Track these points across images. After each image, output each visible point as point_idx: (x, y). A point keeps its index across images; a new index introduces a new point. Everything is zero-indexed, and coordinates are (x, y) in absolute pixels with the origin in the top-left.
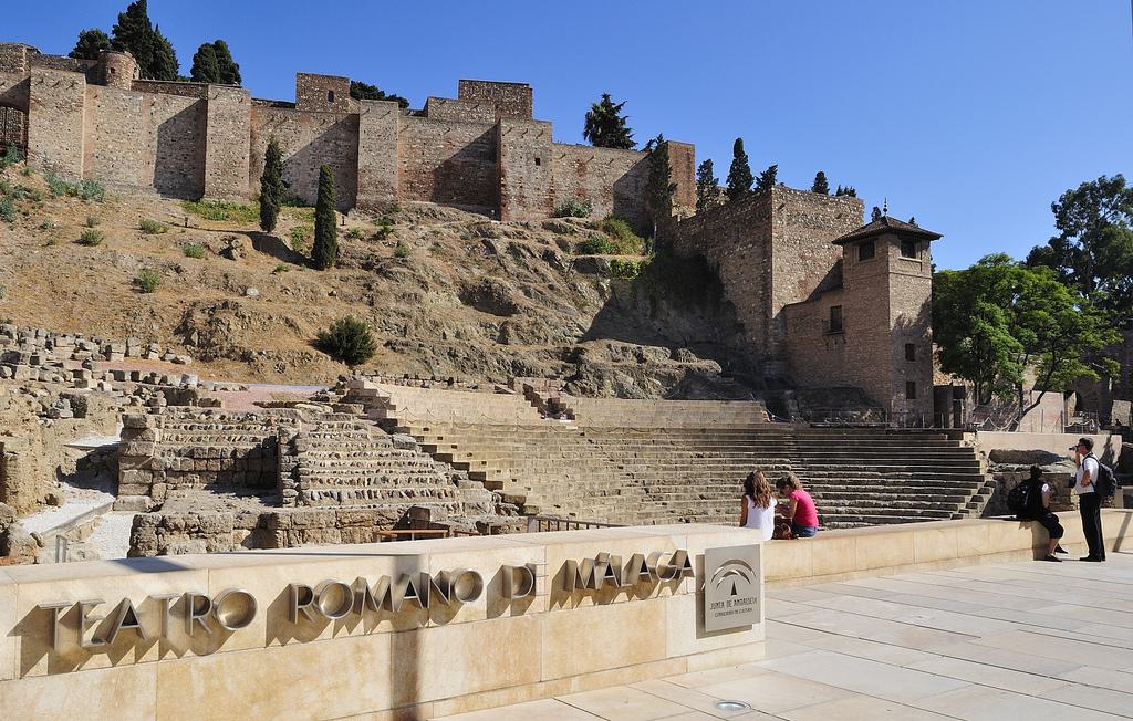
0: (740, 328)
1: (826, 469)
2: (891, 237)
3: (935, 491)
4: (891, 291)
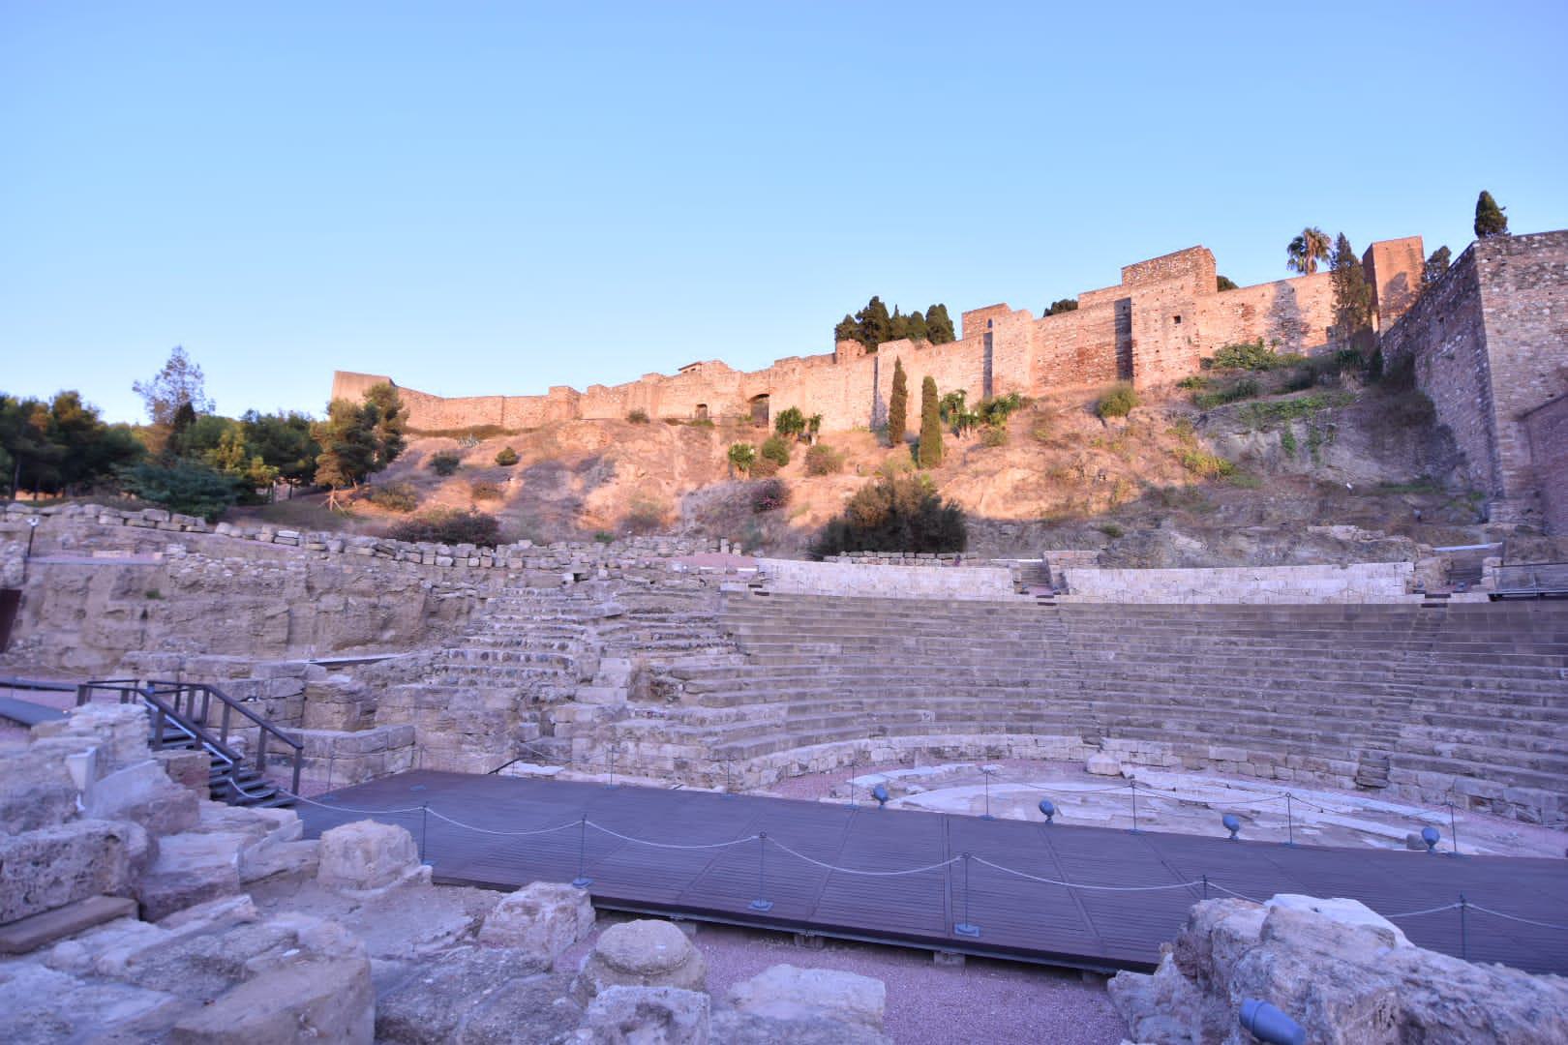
0: (1461, 460)
1: (1463, 672)
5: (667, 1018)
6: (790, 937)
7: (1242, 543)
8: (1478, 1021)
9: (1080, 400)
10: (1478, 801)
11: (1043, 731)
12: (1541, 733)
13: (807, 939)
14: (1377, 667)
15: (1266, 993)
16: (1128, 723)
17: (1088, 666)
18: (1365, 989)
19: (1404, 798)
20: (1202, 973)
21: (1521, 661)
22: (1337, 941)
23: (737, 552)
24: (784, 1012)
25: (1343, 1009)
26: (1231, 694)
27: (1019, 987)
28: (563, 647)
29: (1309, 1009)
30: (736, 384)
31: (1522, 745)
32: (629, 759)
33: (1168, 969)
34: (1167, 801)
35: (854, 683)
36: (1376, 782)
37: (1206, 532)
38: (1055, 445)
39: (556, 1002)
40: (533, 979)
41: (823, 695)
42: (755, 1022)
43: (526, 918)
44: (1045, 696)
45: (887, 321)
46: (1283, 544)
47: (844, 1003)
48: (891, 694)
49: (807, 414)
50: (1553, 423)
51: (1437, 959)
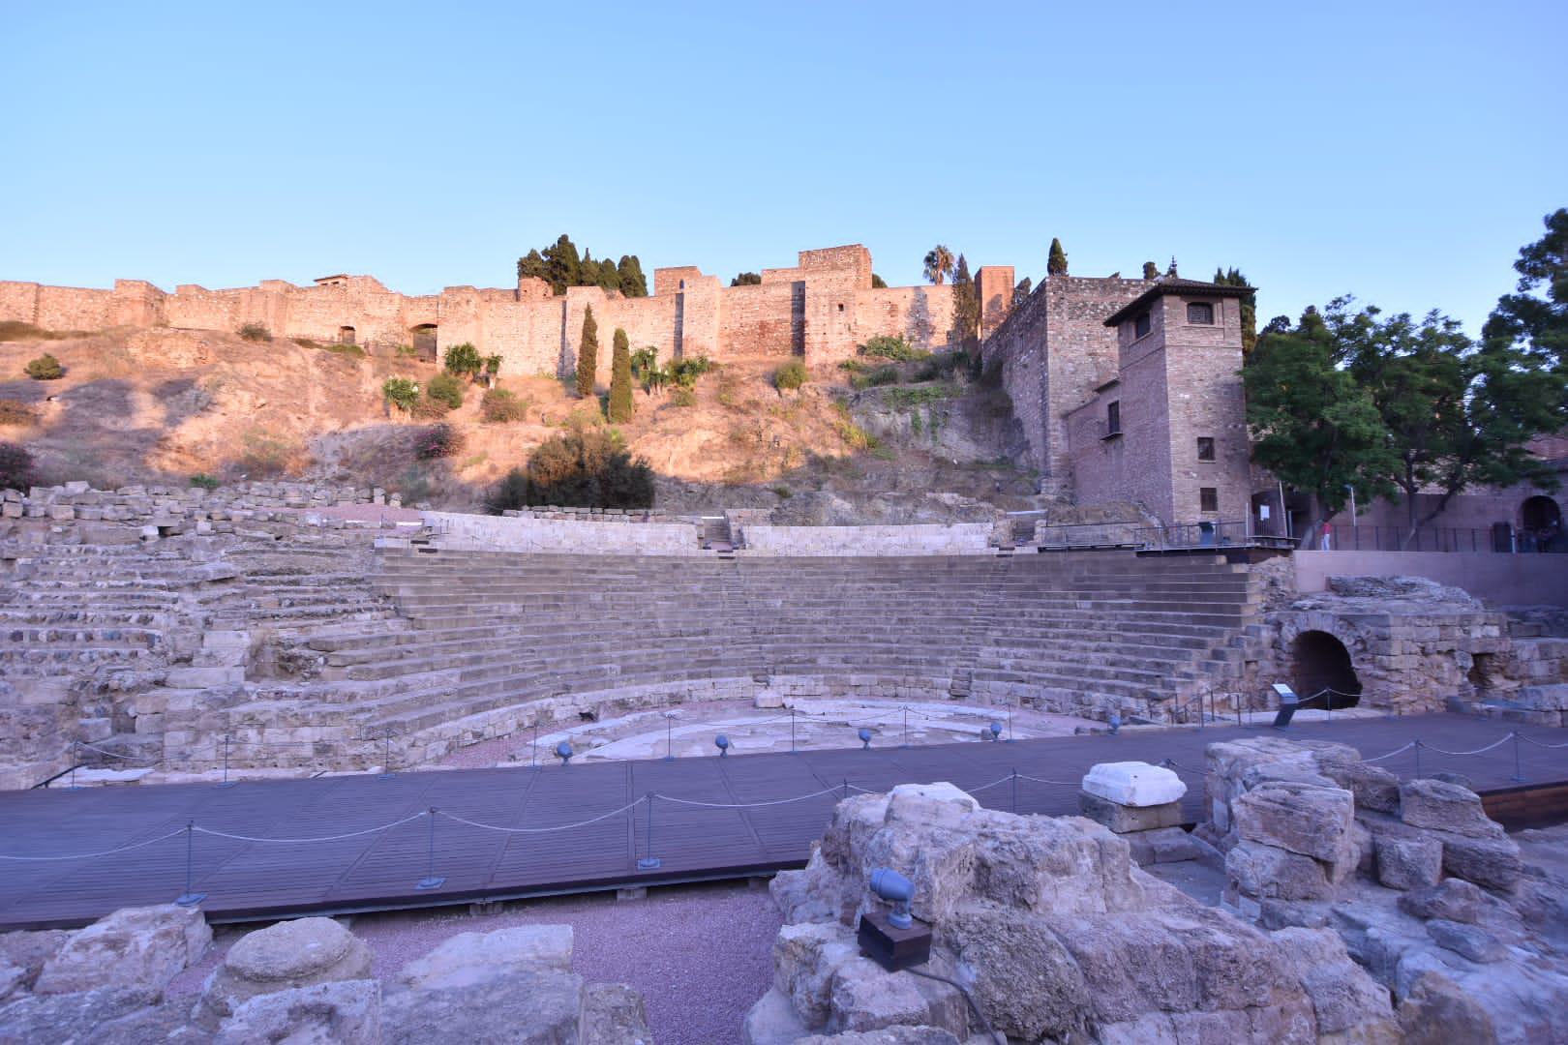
0: (1026, 446)
1: (1020, 605)
2: (1177, 299)
3: (1156, 641)
4: (1171, 370)
5: (329, 1014)
6: (464, 909)
7: (881, 505)
8: (1022, 856)
9: (761, 369)
10: (1025, 700)
11: (721, 675)
12: (1064, 648)
13: (484, 907)
14: (966, 604)
15: (889, 863)
16: (790, 661)
17: (760, 613)
18: (954, 846)
19: (980, 703)
20: (842, 860)
21: (1055, 596)
22: (936, 814)
23: (396, 503)
24: (466, 979)
25: (940, 863)
26: (868, 631)
27: (693, 906)
28: (145, 621)
29: (917, 868)
30: (396, 306)
31: (1052, 657)
32: (250, 750)
33: (817, 862)
34: (818, 725)
35: (537, 642)
36: (964, 692)
37: (853, 495)
38: (738, 410)
39: (174, 1034)
40: (132, 1017)
41: (501, 658)
42: (432, 996)
43: (110, 954)
44: (723, 642)
45: (577, 263)
46: (910, 507)
47: (530, 955)
48: (577, 651)
49: (484, 352)
50: (1082, 423)
51: (1000, 816)
